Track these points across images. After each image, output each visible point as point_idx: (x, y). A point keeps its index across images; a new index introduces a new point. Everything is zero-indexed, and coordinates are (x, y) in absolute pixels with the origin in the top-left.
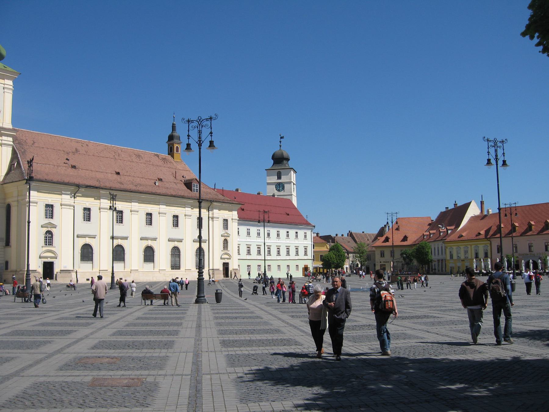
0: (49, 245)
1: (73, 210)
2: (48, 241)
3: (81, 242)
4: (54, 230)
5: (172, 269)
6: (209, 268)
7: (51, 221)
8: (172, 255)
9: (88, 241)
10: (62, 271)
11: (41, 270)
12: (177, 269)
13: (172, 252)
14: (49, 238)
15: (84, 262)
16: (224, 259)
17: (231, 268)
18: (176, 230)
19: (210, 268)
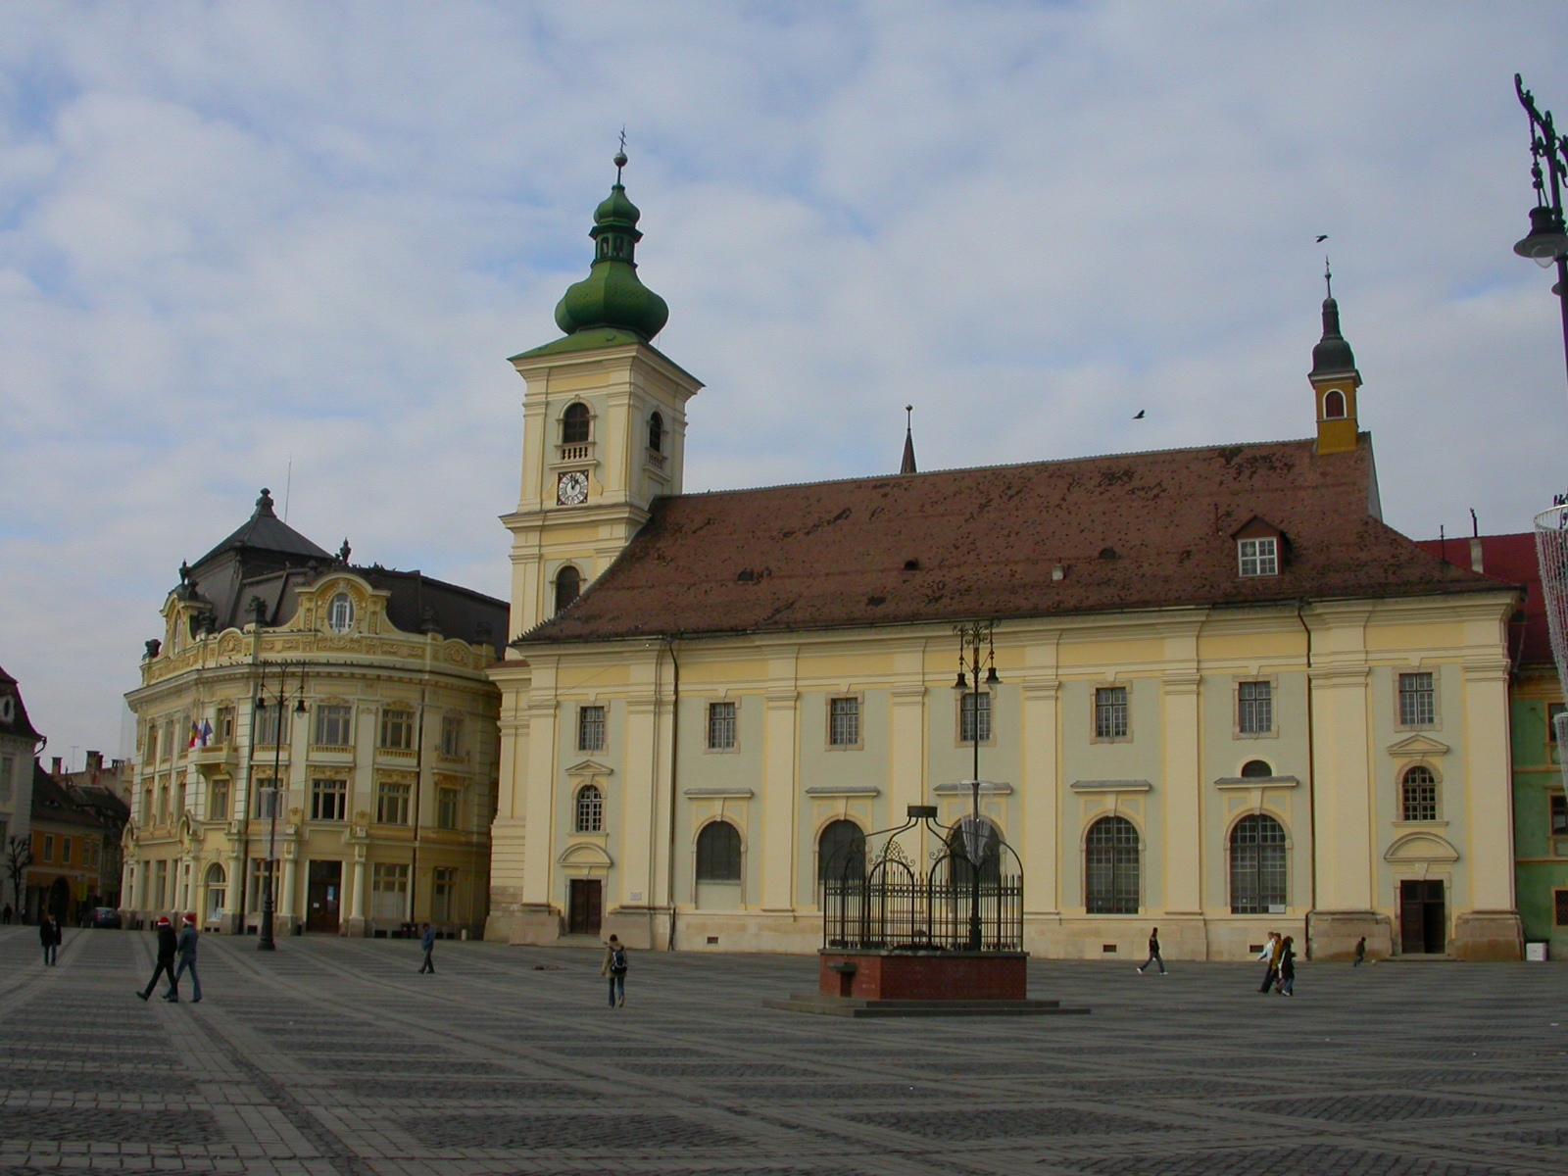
0: (594, 828)
1: (671, 716)
2: (591, 817)
3: (695, 818)
4: (602, 783)
5: (1090, 910)
6: (1314, 905)
7: (597, 757)
8: (1092, 854)
9: (715, 811)
10: (625, 910)
11: (562, 903)
12: (1128, 911)
13: (1089, 840)
14: (588, 810)
15: (712, 881)
16: (1411, 861)
17: (1457, 907)
18: (1107, 749)
19: (1319, 908)
